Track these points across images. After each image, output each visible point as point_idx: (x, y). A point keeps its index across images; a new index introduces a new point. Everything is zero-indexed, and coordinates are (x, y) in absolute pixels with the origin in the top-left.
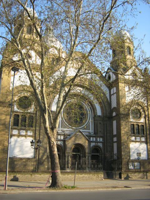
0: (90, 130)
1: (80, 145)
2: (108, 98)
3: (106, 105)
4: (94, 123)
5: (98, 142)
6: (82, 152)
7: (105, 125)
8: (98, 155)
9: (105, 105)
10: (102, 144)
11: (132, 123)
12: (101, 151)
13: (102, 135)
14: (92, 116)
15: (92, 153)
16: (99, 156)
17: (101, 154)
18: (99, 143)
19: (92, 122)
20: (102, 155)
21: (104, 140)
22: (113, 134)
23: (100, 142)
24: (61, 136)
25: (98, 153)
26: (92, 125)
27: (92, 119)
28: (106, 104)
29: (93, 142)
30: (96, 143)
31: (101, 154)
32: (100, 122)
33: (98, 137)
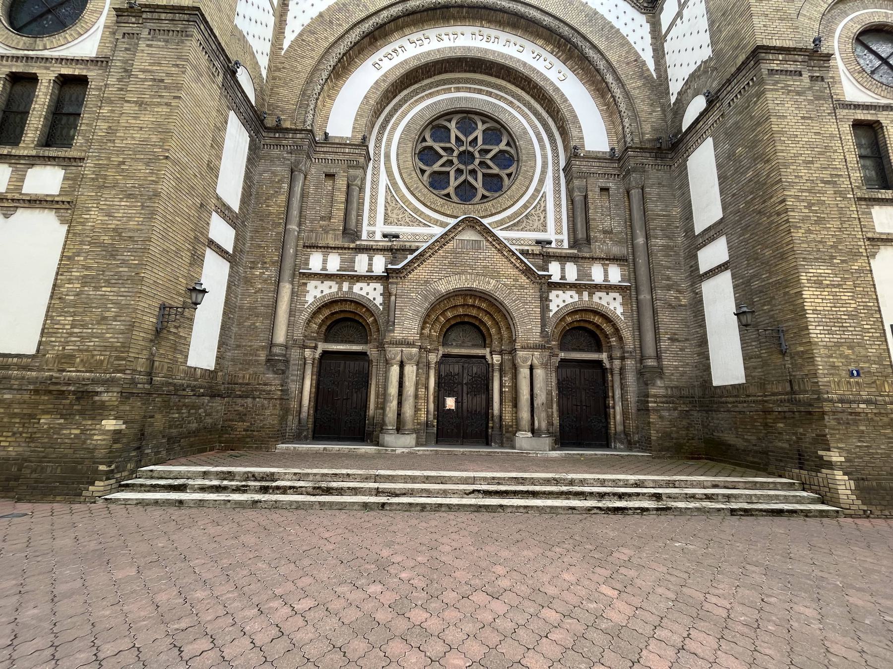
0: (545, 231)
1: (484, 305)
2: (648, 57)
3: (635, 93)
4: (571, 200)
5: (598, 287)
6: (501, 339)
7: (635, 193)
8: (599, 363)
9: (627, 94)
10: (619, 298)
11: (861, 115)
12: (620, 339)
13: (616, 250)
14: (556, 163)
15: (563, 347)
16: (604, 370)
17: (617, 353)
18: (602, 294)
19: (557, 192)
20: (623, 358)
21: (633, 274)
22: (689, 228)
23: (608, 288)
24: (371, 259)
25: (599, 350)
26: (558, 205)
27: (556, 179)
28: (639, 83)
29: (562, 286)
30: (585, 294)
31: (617, 353)
32: (602, 182)
33: (594, 259)
